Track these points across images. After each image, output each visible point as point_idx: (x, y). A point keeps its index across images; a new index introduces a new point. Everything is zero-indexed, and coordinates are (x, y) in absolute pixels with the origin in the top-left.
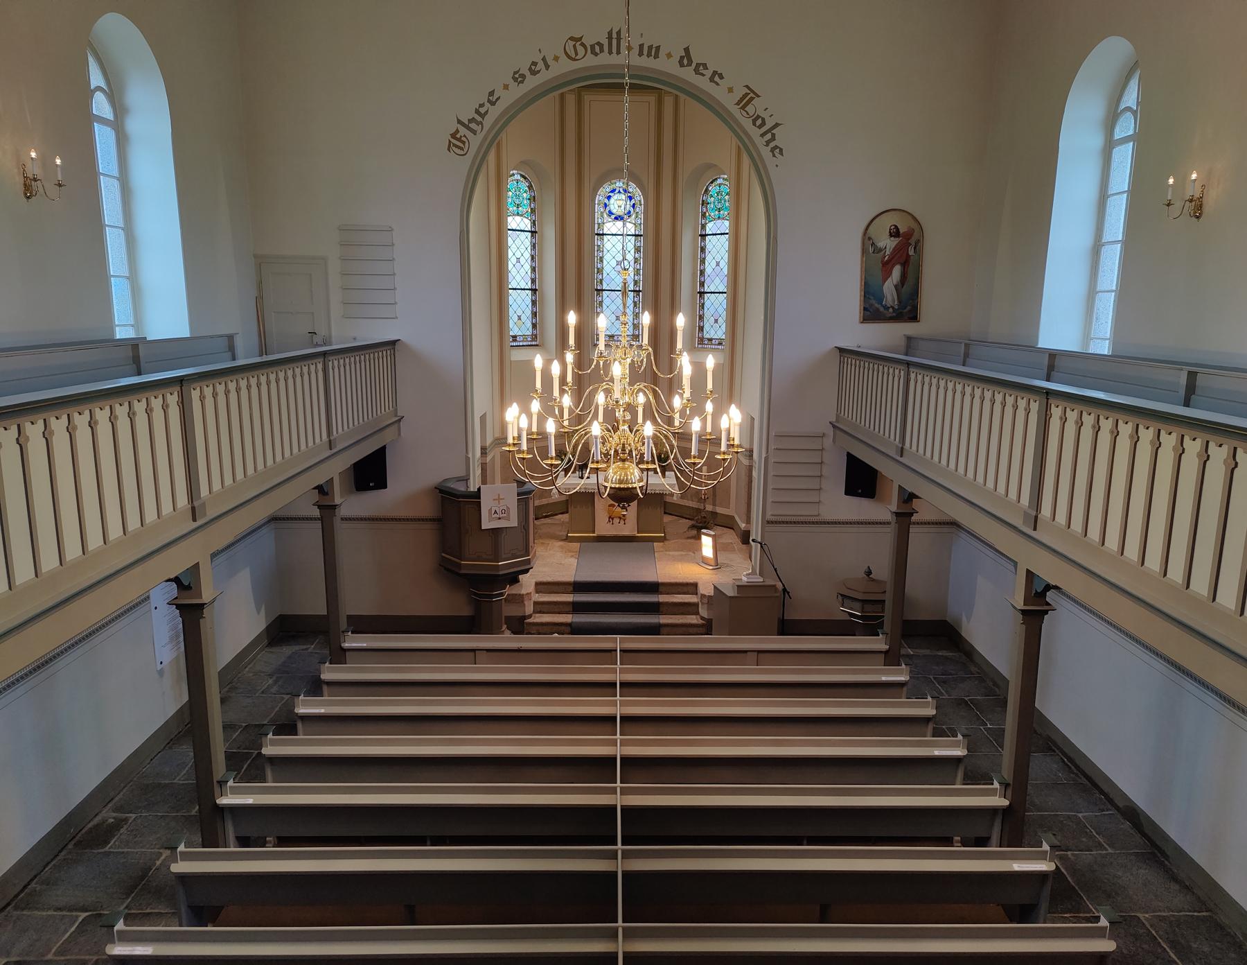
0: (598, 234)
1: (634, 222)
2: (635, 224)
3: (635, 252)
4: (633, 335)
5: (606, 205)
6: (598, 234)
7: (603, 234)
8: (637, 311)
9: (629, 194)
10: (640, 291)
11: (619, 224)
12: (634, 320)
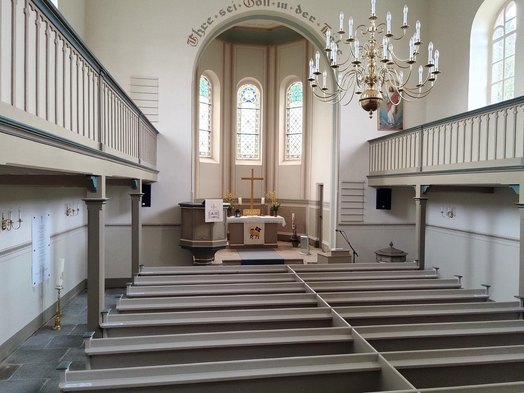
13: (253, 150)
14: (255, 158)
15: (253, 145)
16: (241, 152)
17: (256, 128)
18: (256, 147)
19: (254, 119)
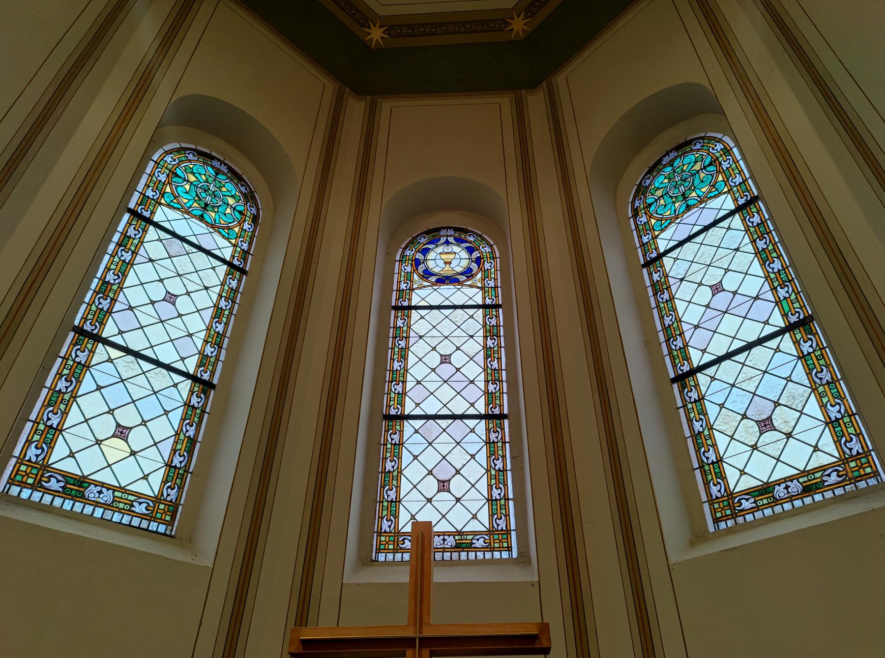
0: (397, 308)
1: (480, 285)
2: (482, 288)
3: (485, 337)
4: (491, 532)
5: (417, 263)
6: (397, 308)
7: (410, 308)
8: (499, 464)
9: (468, 245)
10: (502, 417)
11: (447, 290)
12: (490, 487)
13: (477, 501)
14: (492, 550)
15: (476, 471)
17: (491, 387)
18: (493, 481)
19: (475, 347)
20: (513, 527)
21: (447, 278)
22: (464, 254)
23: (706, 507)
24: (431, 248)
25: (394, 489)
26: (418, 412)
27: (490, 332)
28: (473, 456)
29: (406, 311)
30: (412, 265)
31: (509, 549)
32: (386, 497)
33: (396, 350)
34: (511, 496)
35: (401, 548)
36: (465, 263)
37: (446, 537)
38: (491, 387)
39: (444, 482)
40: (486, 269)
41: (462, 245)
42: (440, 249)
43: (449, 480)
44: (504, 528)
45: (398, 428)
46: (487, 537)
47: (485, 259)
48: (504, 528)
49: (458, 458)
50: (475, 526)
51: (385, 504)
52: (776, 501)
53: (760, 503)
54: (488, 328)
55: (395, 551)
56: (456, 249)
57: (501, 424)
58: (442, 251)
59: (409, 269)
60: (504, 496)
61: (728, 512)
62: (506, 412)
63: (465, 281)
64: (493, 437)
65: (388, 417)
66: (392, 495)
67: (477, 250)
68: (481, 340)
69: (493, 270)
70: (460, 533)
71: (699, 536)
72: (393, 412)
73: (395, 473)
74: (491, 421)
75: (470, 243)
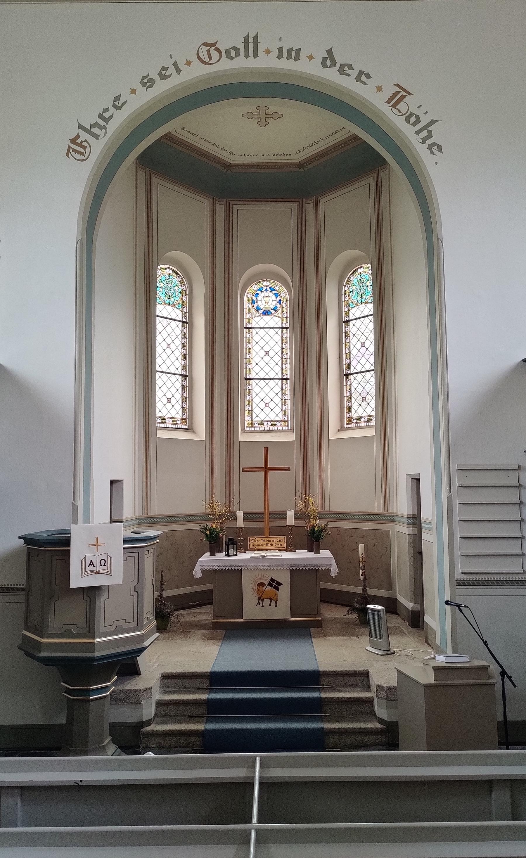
0: (246, 328)
1: (280, 316)
4: (282, 421)
5: (253, 302)
6: (246, 328)
8: (286, 397)
9: (276, 292)
10: (287, 379)
11: (267, 318)
13: (278, 410)
14: (282, 426)
15: (277, 400)
16: (254, 416)
17: (284, 367)
20: (289, 419)
21: (267, 311)
22: (274, 298)
23: (345, 419)
24: (259, 293)
25: (250, 406)
26: (257, 377)
27: (284, 341)
28: (277, 394)
29: (250, 330)
30: (251, 303)
31: (288, 426)
32: (248, 409)
33: (247, 349)
34: (289, 409)
35: (254, 426)
36: (274, 303)
37: (268, 422)
38: (284, 367)
39: (267, 403)
40: (283, 307)
41: (273, 292)
42: (263, 294)
43: (269, 403)
44: (287, 420)
45: (250, 383)
46: (281, 422)
47: (283, 301)
48: (287, 420)
49: (272, 395)
50: (277, 419)
51: (248, 411)
52: (361, 422)
53: (357, 422)
54: (283, 339)
55: (252, 427)
56: (271, 294)
57: (287, 382)
58: (264, 296)
59: (250, 306)
60: (287, 409)
61: (350, 422)
62: (289, 377)
63: (274, 313)
64: (284, 387)
65: (246, 379)
66: (250, 408)
67: (280, 295)
68: (280, 345)
69: (286, 308)
70: (272, 421)
71: (342, 429)
72: (248, 377)
73: (250, 400)
74: (283, 381)
75: (277, 291)
